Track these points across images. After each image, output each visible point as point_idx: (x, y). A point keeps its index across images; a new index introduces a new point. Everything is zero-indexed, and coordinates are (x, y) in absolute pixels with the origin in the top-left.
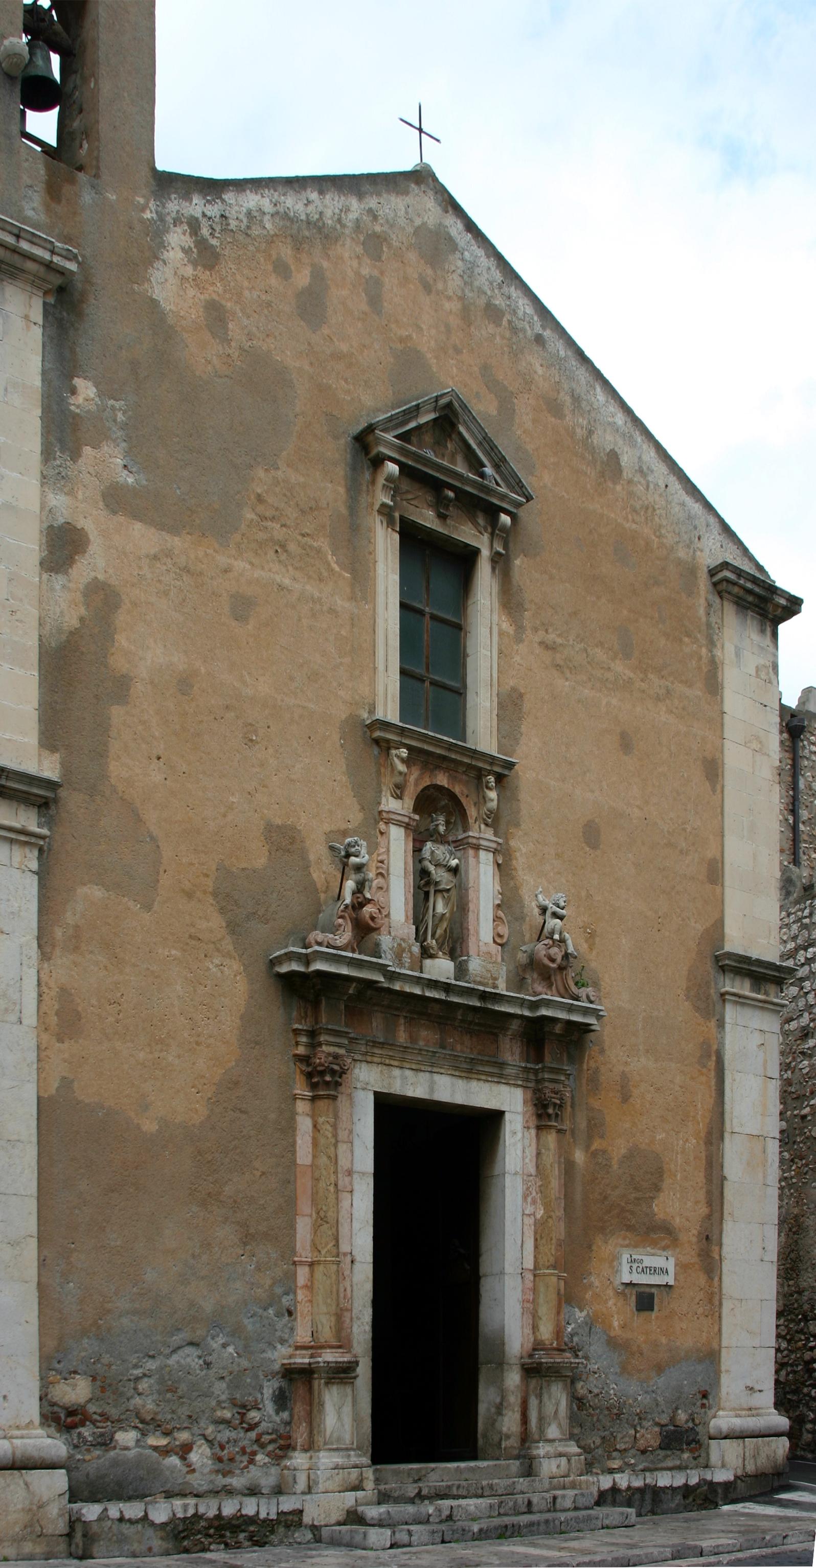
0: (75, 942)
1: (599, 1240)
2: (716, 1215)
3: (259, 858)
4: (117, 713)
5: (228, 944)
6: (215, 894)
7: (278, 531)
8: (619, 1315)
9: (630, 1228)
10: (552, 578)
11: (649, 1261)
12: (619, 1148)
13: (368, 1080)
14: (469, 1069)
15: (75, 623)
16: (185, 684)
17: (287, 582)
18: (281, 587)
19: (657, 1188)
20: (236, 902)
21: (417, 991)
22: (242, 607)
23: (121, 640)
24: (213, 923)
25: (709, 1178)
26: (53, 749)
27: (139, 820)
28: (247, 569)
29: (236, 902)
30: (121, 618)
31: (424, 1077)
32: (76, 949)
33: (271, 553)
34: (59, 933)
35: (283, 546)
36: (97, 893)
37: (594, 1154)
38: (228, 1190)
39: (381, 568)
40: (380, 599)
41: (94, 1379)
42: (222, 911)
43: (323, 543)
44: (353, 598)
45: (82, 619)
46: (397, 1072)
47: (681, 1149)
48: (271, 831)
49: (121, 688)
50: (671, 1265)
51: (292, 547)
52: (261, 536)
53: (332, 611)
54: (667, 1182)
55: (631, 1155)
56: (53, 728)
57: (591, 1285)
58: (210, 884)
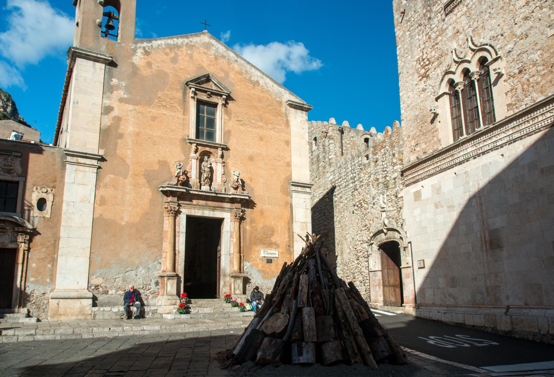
0: (106, 186)
1: (254, 246)
2: (291, 241)
3: (156, 167)
4: (119, 141)
5: (147, 185)
6: (144, 175)
7: (164, 103)
8: (261, 264)
9: (263, 244)
10: (240, 107)
11: (269, 251)
12: (260, 225)
13: (185, 211)
14: (214, 209)
15: (110, 124)
16: (138, 134)
17: (166, 113)
18: (164, 114)
19: (272, 235)
20: (149, 176)
21: (197, 193)
22: (154, 118)
23: (122, 127)
24: (143, 181)
25: (289, 232)
26: (102, 149)
27: (124, 161)
28: (154, 111)
29: (149, 176)
30: (122, 123)
31: (200, 211)
32: (106, 187)
33: (162, 108)
34: (101, 184)
35: (165, 106)
36: (112, 176)
37: (252, 227)
38: (144, 236)
39: (191, 109)
40: (191, 115)
41: (104, 278)
42: (146, 178)
43: (176, 105)
44: (184, 115)
45: (112, 124)
46: (193, 210)
47: (281, 226)
48: (159, 162)
49: (121, 136)
50: (277, 252)
51: (168, 106)
52: (159, 105)
53: (178, 118)
54: (275, 233)
55: (264, 227)
56: (102, 144)
57: (252, 257)
58: (143, 173)
